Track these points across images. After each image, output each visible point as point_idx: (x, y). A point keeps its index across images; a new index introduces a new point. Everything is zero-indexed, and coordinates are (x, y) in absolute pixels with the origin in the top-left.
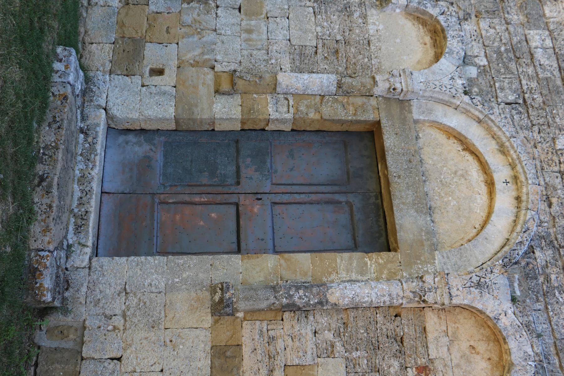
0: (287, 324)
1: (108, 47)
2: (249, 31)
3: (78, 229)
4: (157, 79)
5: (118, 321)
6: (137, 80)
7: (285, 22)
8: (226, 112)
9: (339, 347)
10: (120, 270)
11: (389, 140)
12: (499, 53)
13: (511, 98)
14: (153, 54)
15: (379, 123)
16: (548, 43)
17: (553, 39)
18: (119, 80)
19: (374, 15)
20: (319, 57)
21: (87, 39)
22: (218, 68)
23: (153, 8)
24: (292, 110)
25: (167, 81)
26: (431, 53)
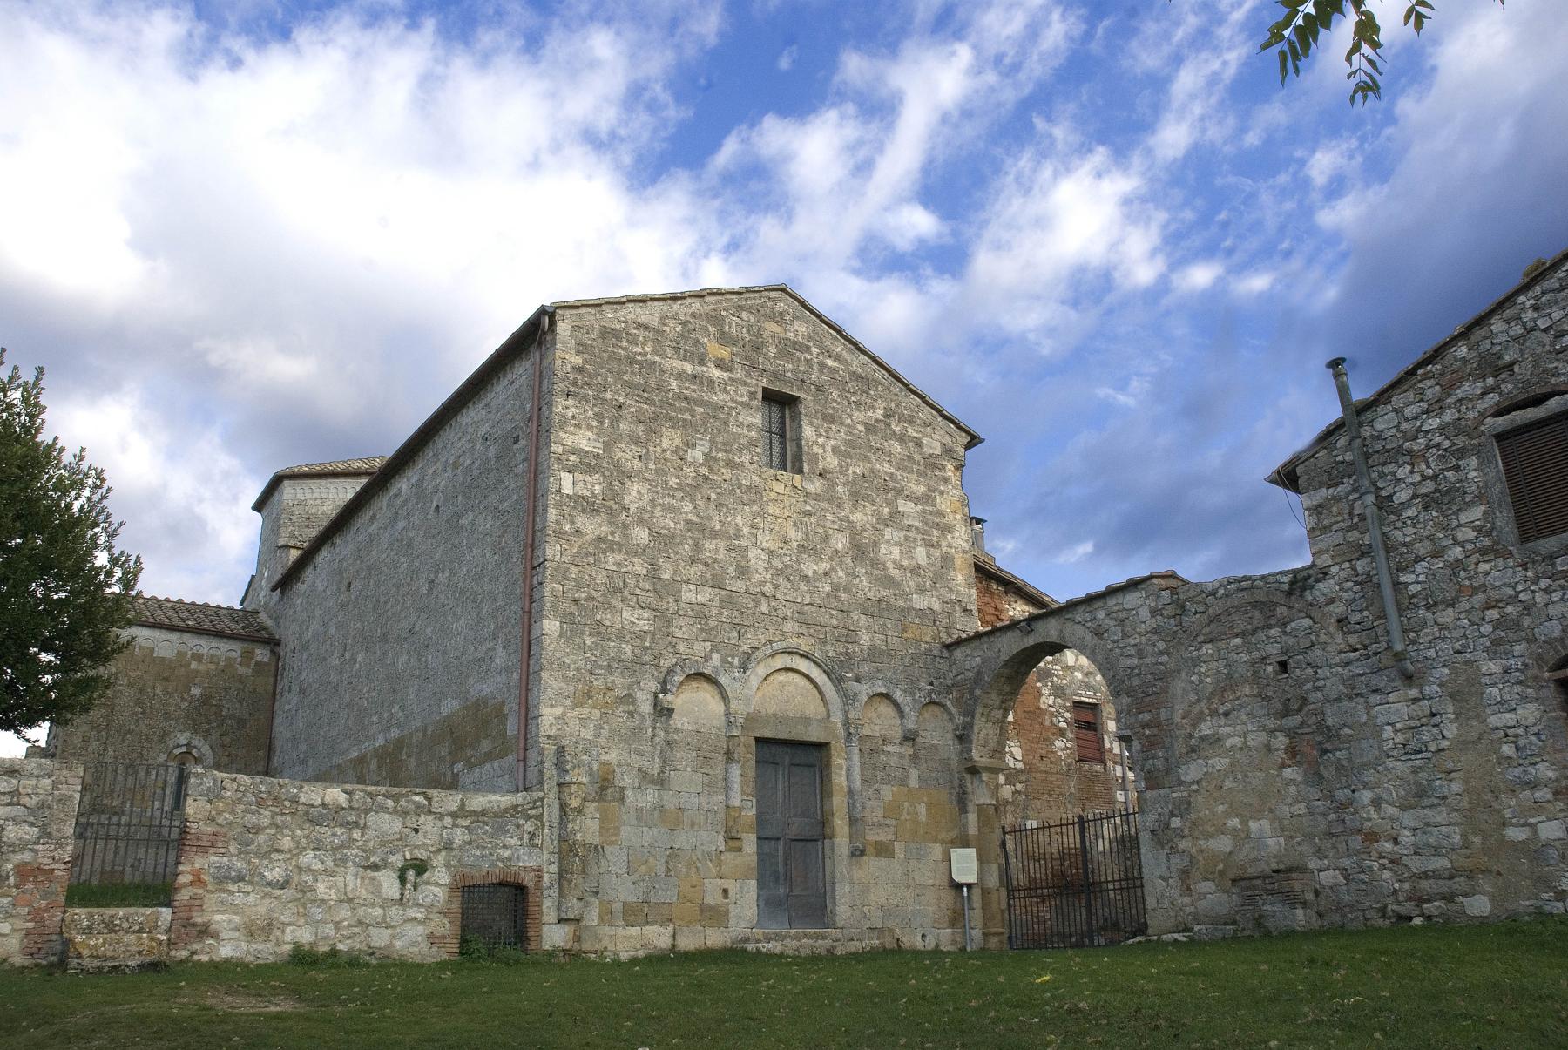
1: (709, 931)
2: (693, 824)
3: (824, 938)
4: (731, 893)
6: (732, 907)
8: (750, 844)
10: (843, 910)
11: (767, 734)
14: (713, 897)
16: (693, 587)
17: (688, 582)
22: (722, 848)
25: (732, 886)
26: (705, 685)
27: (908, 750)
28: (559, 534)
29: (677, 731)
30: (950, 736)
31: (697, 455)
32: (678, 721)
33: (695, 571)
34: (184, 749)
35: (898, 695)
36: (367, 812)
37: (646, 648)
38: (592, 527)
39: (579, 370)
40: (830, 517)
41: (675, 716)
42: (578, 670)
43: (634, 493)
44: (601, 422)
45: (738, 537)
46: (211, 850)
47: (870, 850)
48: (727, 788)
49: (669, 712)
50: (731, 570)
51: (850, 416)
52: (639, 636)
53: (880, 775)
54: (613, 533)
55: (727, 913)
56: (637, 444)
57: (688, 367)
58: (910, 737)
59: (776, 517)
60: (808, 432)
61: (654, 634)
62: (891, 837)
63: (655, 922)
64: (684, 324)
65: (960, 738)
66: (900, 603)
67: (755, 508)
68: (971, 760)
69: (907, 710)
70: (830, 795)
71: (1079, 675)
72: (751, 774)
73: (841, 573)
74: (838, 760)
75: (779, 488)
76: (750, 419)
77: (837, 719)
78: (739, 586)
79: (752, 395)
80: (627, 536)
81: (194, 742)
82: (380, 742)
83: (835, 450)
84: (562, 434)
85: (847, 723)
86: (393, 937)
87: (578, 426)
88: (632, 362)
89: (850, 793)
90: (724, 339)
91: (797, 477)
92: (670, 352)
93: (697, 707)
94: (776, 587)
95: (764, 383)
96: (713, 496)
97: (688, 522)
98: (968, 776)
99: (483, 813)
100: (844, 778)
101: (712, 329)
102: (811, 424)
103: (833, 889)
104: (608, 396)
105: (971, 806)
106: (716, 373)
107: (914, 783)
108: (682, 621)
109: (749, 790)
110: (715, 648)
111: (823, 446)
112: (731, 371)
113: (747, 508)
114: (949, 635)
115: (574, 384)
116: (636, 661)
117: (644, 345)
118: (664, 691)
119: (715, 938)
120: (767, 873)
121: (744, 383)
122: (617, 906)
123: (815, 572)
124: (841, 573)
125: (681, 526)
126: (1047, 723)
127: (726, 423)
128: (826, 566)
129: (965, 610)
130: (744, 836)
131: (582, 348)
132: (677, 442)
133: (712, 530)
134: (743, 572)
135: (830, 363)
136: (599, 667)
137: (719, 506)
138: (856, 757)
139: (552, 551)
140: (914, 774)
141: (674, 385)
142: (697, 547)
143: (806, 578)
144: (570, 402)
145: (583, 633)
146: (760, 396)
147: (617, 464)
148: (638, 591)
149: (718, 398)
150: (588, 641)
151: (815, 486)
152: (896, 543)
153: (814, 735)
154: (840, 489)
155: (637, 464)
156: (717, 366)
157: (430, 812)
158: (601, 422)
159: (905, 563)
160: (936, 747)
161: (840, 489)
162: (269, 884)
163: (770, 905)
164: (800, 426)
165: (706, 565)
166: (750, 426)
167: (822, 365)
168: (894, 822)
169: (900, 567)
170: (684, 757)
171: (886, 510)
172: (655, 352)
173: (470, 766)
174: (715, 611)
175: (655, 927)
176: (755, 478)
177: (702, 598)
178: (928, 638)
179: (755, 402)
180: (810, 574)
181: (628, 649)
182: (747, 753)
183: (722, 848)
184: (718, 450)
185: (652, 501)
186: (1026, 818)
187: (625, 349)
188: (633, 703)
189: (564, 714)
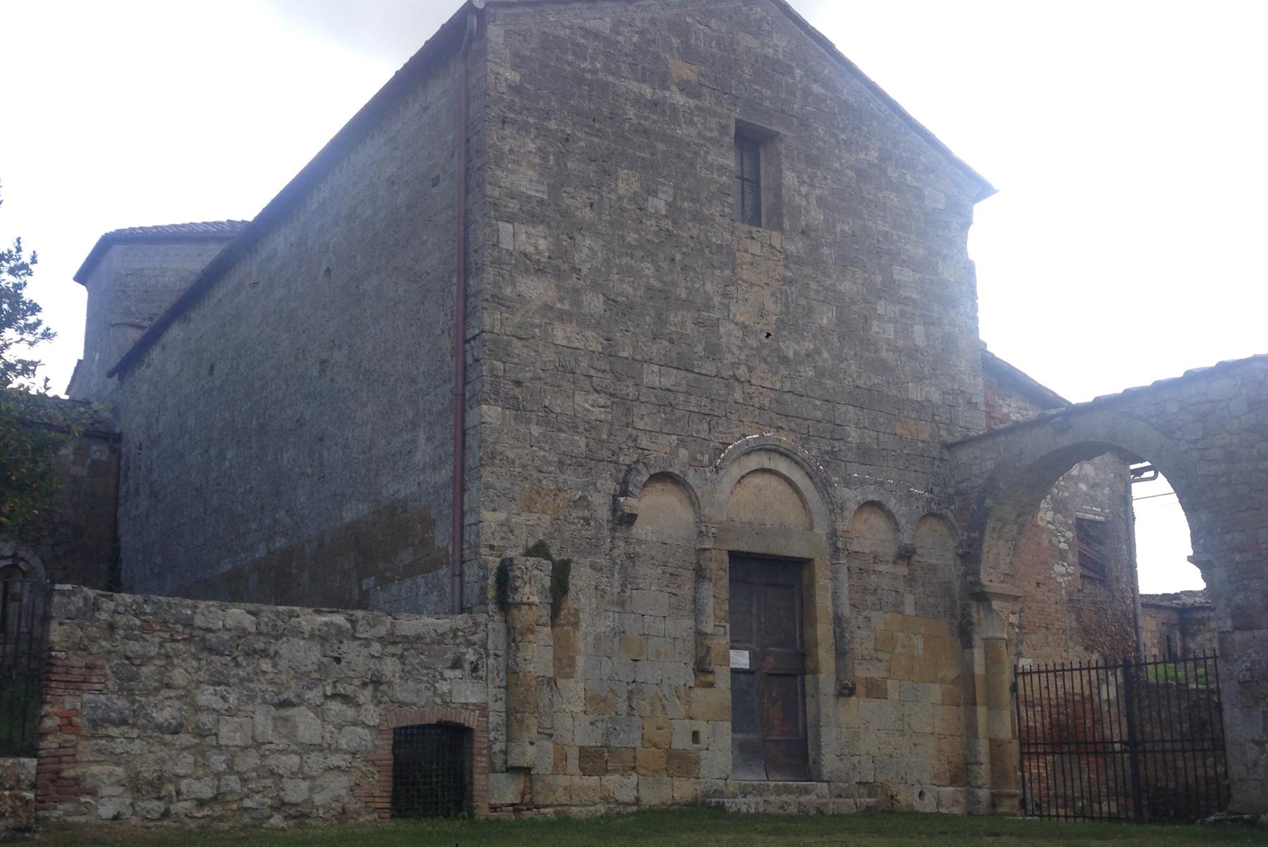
0: (855, 646)
1: (677, 782)
4: (703, 737)
5: (855, 760)
6: (703, 754)
7: (648, 619)
9: (866, 613)
10: (829, 761)
11: (742, 547)
12: (666, 420)
13: (706, 427)
14: (681, 742)
15: (729, 552)
16: (656, 368)
17: (650, 362)
18: (703, 772)
19: (639, 530)
20: (677, 591)
21: (670, 802)
22: (691, 683)
23: (638, 744)
24: (723, 623)
25: (703, 728)
26: (670, 487)
27: (902, 570)
28: (499, 301)
29: (640, 542)
30: (950, 555)
31: (658, 204)
32: (640, 530)
33: (656, 349)
34: (9, 562)
35: (892, 504)
36: (277, 638)
37: (601, 441)
38: (536, 289)
39: (515, 89)
40: (813, 285)
41: (637, 523)
42: (524, 466)
43: (585, 251)
44: (545, 159)
45: (709, 307)
46: (85, 687)
47: (860, 689)
48: (697, 612)
49: (630, 519)
50: (700, 349)
51: (839, 158)
52: (592, 427)
53: (870, 599)
54: (561, 300)
55: (697, 762)
56: (587, 188)
57: (647, 91)
58: (905, 555)
59: (752, 285)
60: (789, 178)
61: (612, 424)
62: (884, 674)
63: (616, 771)
64: (642, 33)
65: (964, 557)
66: (894, 392)
67: (727, 272)
68: (978, 583)
69: (903, 521)
70: (813, 621)
71: (1083, 487)
72: (724, 594)
73: (825, 355)
74: (823, 580)
75: (755, 248)
76: (721, 161)
77: (821, 530)
78: (710, 368)
79: (723, 128)
80: (577, 303)
81: (22, 554)
82: (261, 552)
83: (821, 202)
84: (499, 173)
85: (833, 535)
86: (311, 789)
87: (517, 162)
88: (581, 81)
89: (838, 620)
90: (689, 54)
91: (775, 234)
92: (624, 69)
93: (660, 513)
94: (751, 370)
95: (737, 114)
96: (678, 257)
97: (649, 288)
98: (974, 604)
99: (419, 638)
100: (829, 603)
101: (675, 41)
102: (793, 169)
103: (818, 735)
104: (552, 125)
105: (977, 641)
106: (680, 99)
107: (909, 610)
108: (644, 410)
109: (722, 614)
110: (682, 443)
111: (807, 197)
112: (697, 96)
113: (718, 272)
114: (950, 432)
115: (511, 107)
116: (591, 456)
117: (593, 60)
118: (625, 493)
119: (684, 789)
120: (744, 711)
121: (714, 114)
122: (573, 754)
123: (796, 353)
124: (825, 355)
125: (640, 293)
126: (1046, 543)
127: (692, 165)
128: (809, 346)
129: (970, 403)
130: (716, 668)
131: (519, 61)
132: (636, 187)
133: (678, 298)
134: (714, 351)
135: (816, 88)
136: (549, 463)
137: (685, 268)
138: (843, 576)
139: (490, 320)
140: (909, 599)
141: (631, 113)
142: (660, 320)
143: (785, 360)
144: (507, 131)
145: (529, 421)
146: (732, 131)
147: (566, 214)
148: (592, 372)
149: (682, 132)
150: (536, 430)
151: (797, 247)
152: (890, 320)
153: (797, 549)
154: (826, 251)
155: (588, 214)
156: (682, 90)
157: (356, 638)
158: (545, 159)
159: (900, 343)
160: (933, 568)
161: (826, 251)
162: (159, 727)
163: (746, 753)
164: (780, 171)
165: (672, 342)
166: (721, 169)
167: (807, 92)
168: (887, 656)
169: (895, 349)
170: (647, 573)
171: (879, 278)
172: (606, 69)
173: (384, 581)
174: (681, 398)
175: (616, 777)
176: (727, 235)
177: (667, 382)
178: (926, 436)
179: (727, 139)
180: (790, 354)
181: (582, 441)
182: (718, 567)
183: (691, 683)
184: (683, 199)
185: (607, 262)
186: (1019, 655)
187: (570, 64)
188: (588, 507)
189: (508, 520)
